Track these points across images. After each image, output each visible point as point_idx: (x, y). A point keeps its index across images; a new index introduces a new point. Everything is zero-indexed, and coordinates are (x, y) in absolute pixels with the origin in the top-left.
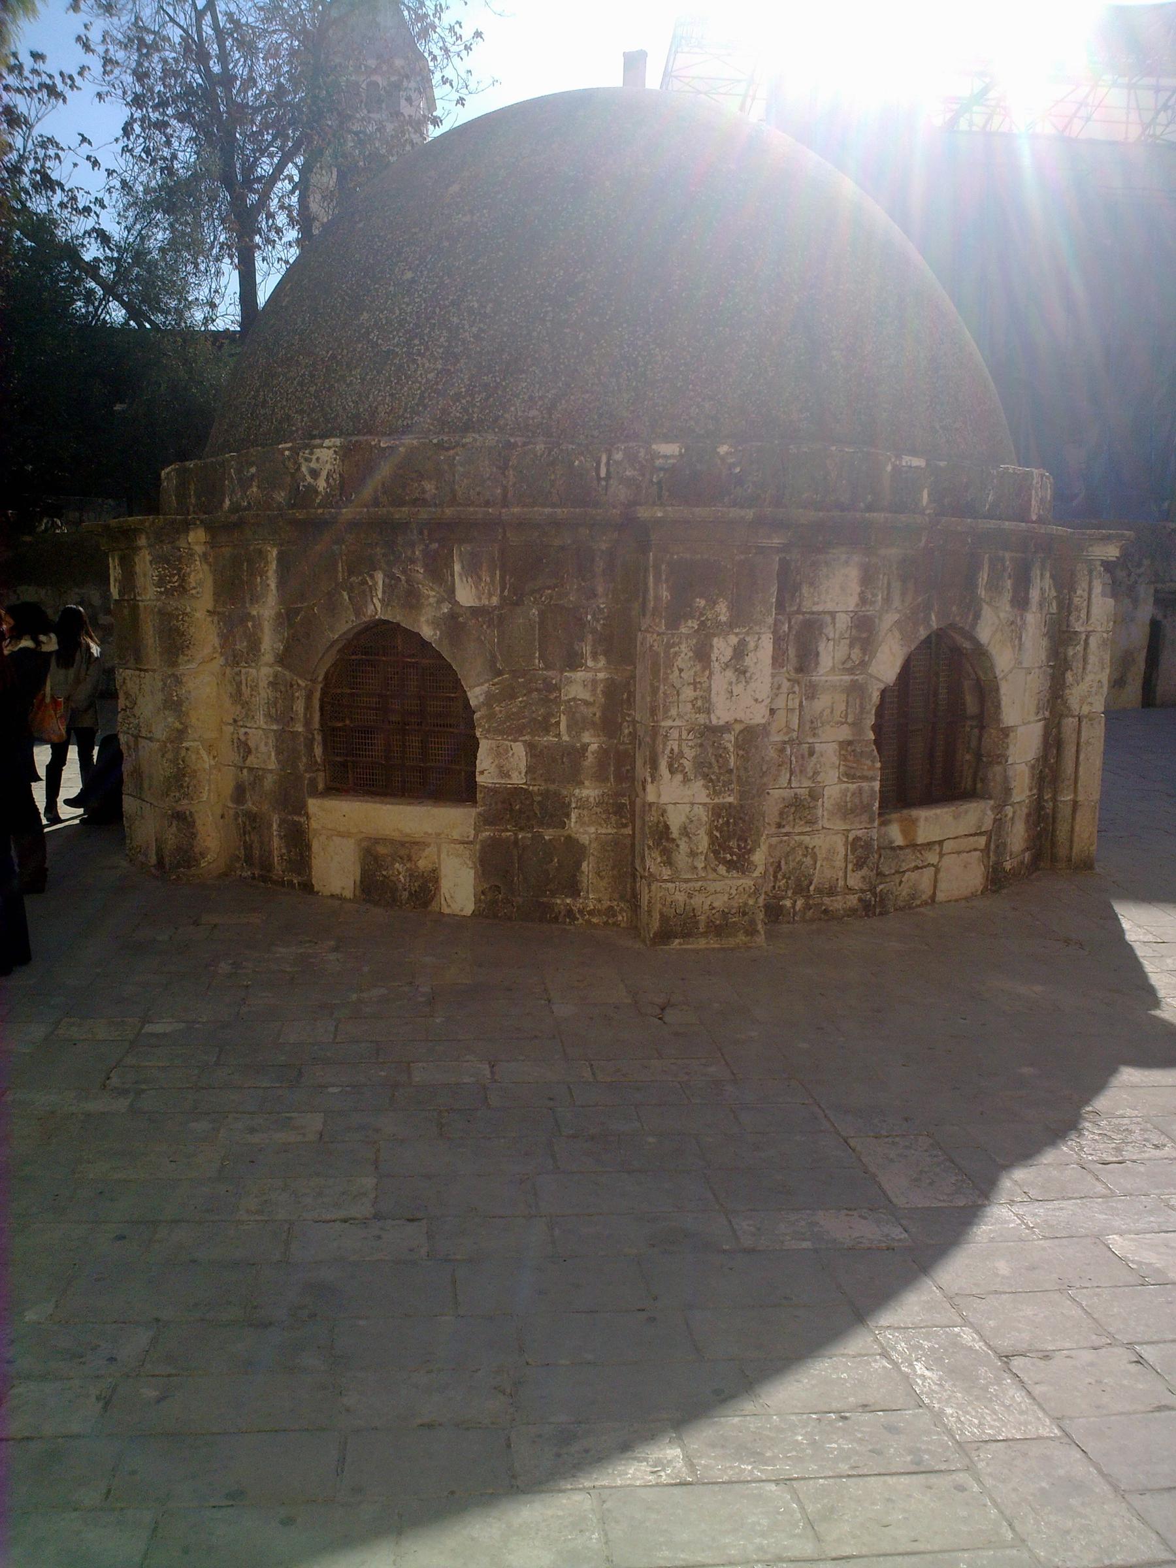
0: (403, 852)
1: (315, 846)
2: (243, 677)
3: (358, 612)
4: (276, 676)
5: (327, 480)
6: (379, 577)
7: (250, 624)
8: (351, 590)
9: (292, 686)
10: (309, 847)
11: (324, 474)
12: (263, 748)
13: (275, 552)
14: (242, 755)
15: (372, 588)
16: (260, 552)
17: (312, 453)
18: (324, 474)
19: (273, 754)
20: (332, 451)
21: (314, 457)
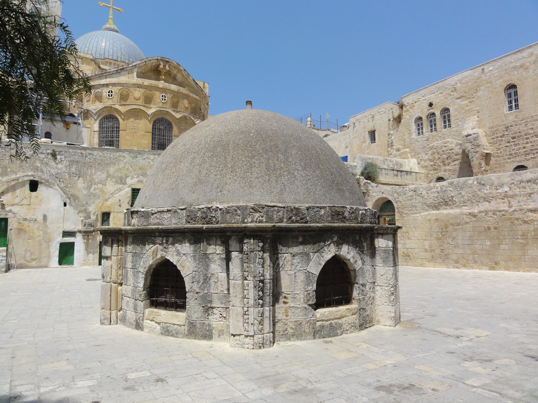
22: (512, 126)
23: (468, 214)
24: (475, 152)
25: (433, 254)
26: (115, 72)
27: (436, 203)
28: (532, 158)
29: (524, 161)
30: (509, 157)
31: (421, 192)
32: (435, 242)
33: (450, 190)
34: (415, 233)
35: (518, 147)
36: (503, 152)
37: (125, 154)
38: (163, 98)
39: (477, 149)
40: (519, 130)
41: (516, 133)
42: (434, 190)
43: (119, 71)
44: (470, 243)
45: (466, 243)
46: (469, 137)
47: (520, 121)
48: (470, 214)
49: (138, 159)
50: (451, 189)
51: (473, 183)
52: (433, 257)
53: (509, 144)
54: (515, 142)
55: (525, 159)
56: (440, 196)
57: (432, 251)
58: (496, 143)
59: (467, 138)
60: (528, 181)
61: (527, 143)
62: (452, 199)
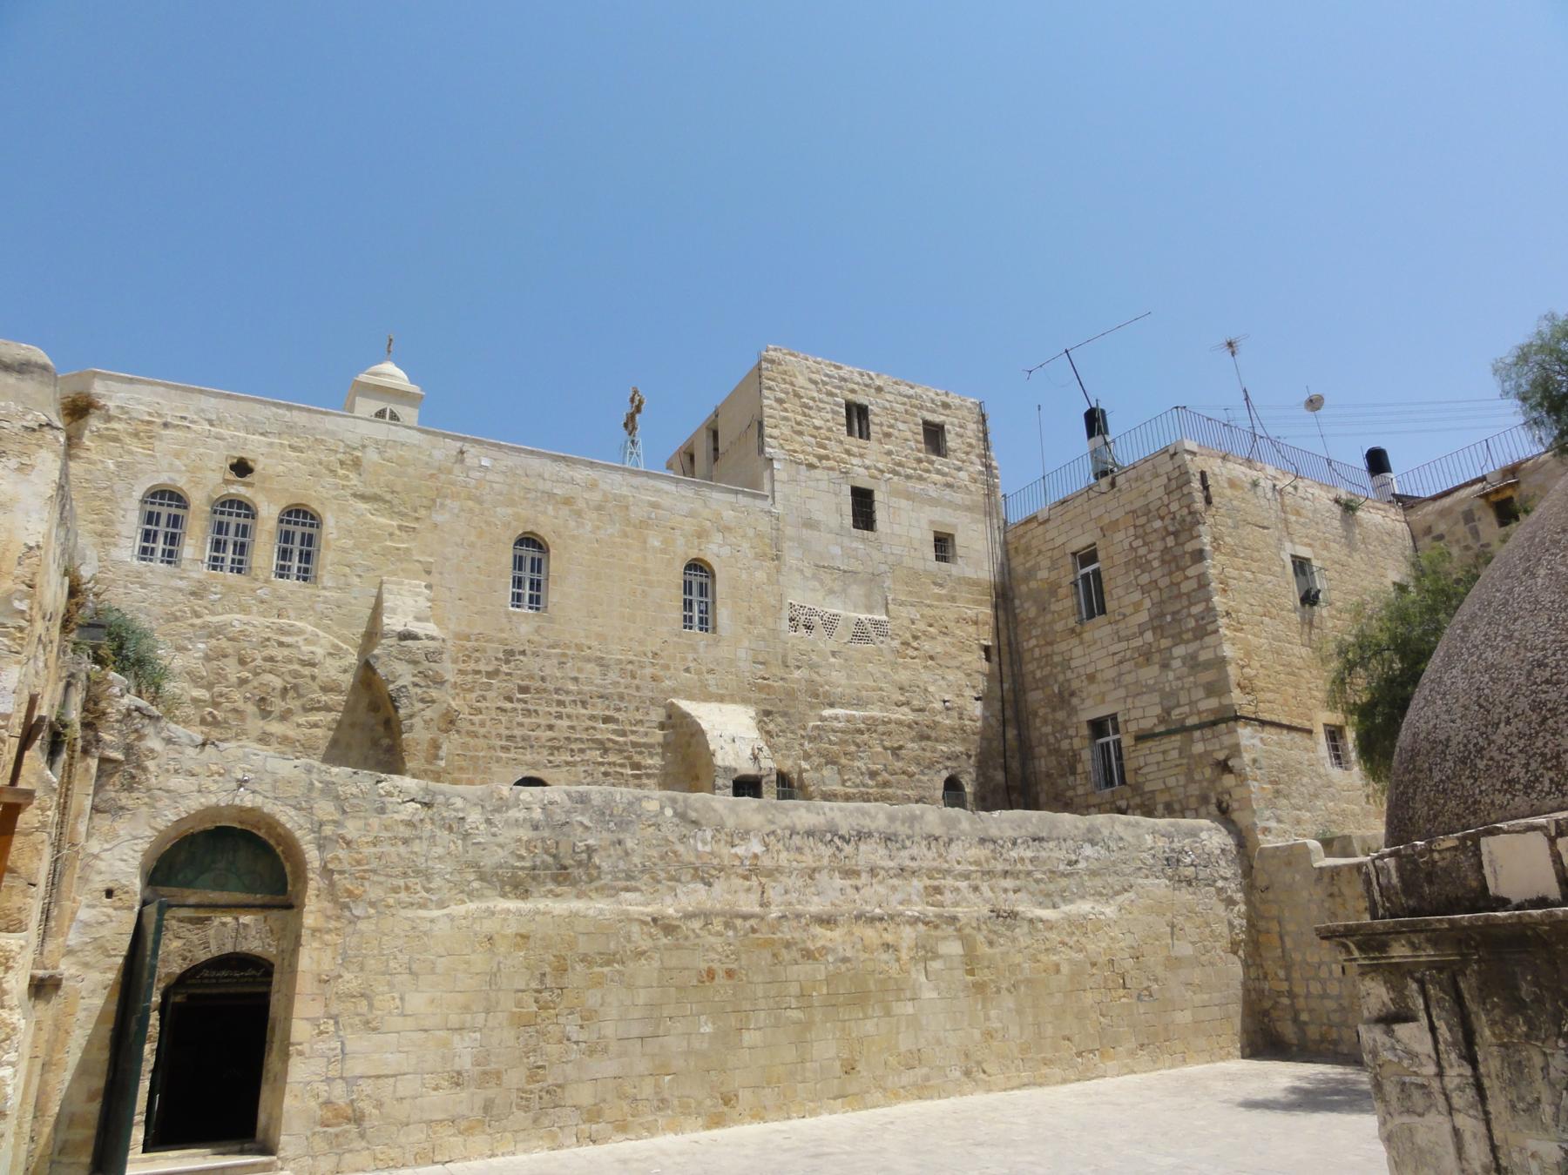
22: (523, 653)
23: (649, 919)
24: (422, 700)
25: (491, 1092)
27: (522, 868)
28: (567, 763)
29: (546, 767)
30: (504, 743)
31: (461, 815)
32: (509, 1035)
33: (581, 824)
34: (407, 997)
35: (534, 720)
36: (488, 723)
39: (434, 693)
40: (541, 670)
41: (531, 677)
42: (514, 813)
44: (649, 1030)
45: (635, 1032)
46: (409, 643)
47: (548, 647)
48: (655, 920)
50: (586, 822)
51: (663, 813)
52: (487, 1107)
53: (508, 705)
54: (526, 702)
55: (550, 762)
56: (543, 840)
57: (490, 1077)
58: (471, 690)
59: (403, 643)
60: (810, 833)
61: (559, 716)
62: (590, 858)
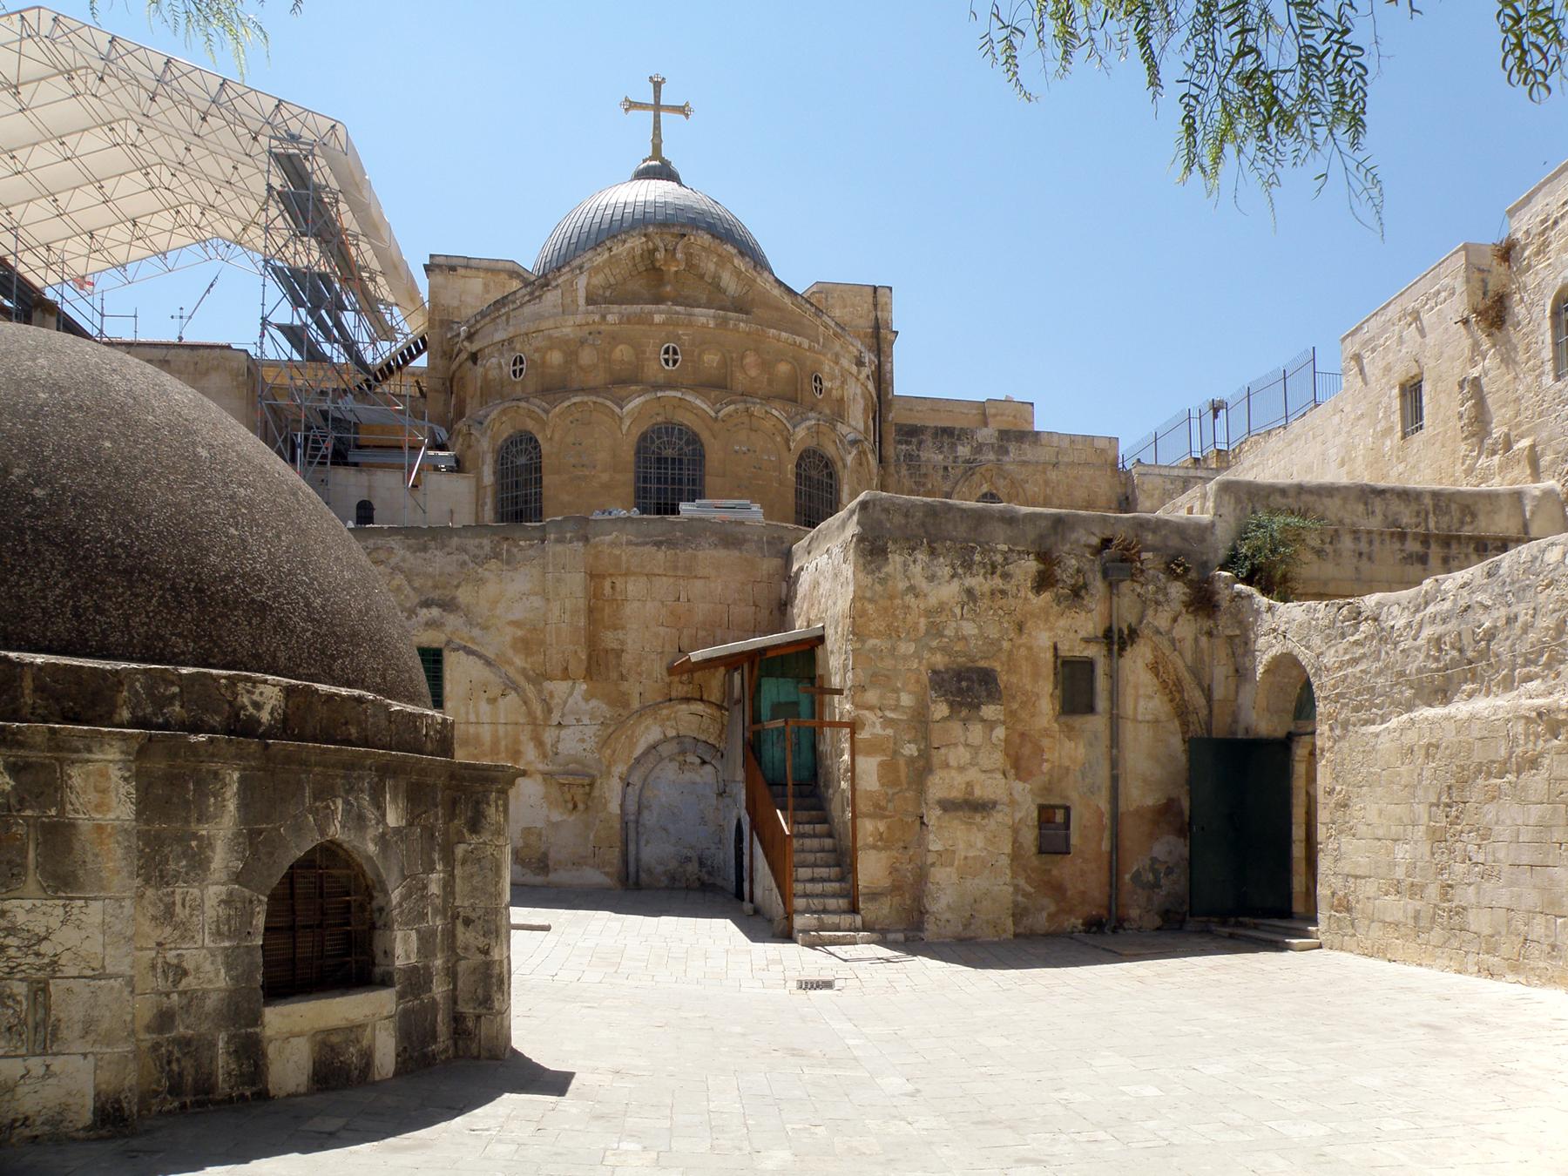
0: (353, 1036)
1: (271, 1050)
2: (178, 898)
3: (323, 832)
4: (230, 894)
5: (271, 713)
6: (339, 802)
7: (194, 844)
8: (315, 812)
9: (251, 902)
10: (264, 1055)
11: (268, 708)
12: (208, 966)
13: (236, 775)
14: (170, 979)
15: (334, 812)
16: (216, 774)
17: (254, 687)
18: (268, 708)
19: (223, 971)
20: (277, 689)
21: (257, 691)
26: (527, 298)
33: (1481, 604)
37: (393, 544)
38: (670, 356)
43: (537, 294)
44: (1538, 858)
45: (1525, 859)
48: (1540, 715)
49: (428, 555)
